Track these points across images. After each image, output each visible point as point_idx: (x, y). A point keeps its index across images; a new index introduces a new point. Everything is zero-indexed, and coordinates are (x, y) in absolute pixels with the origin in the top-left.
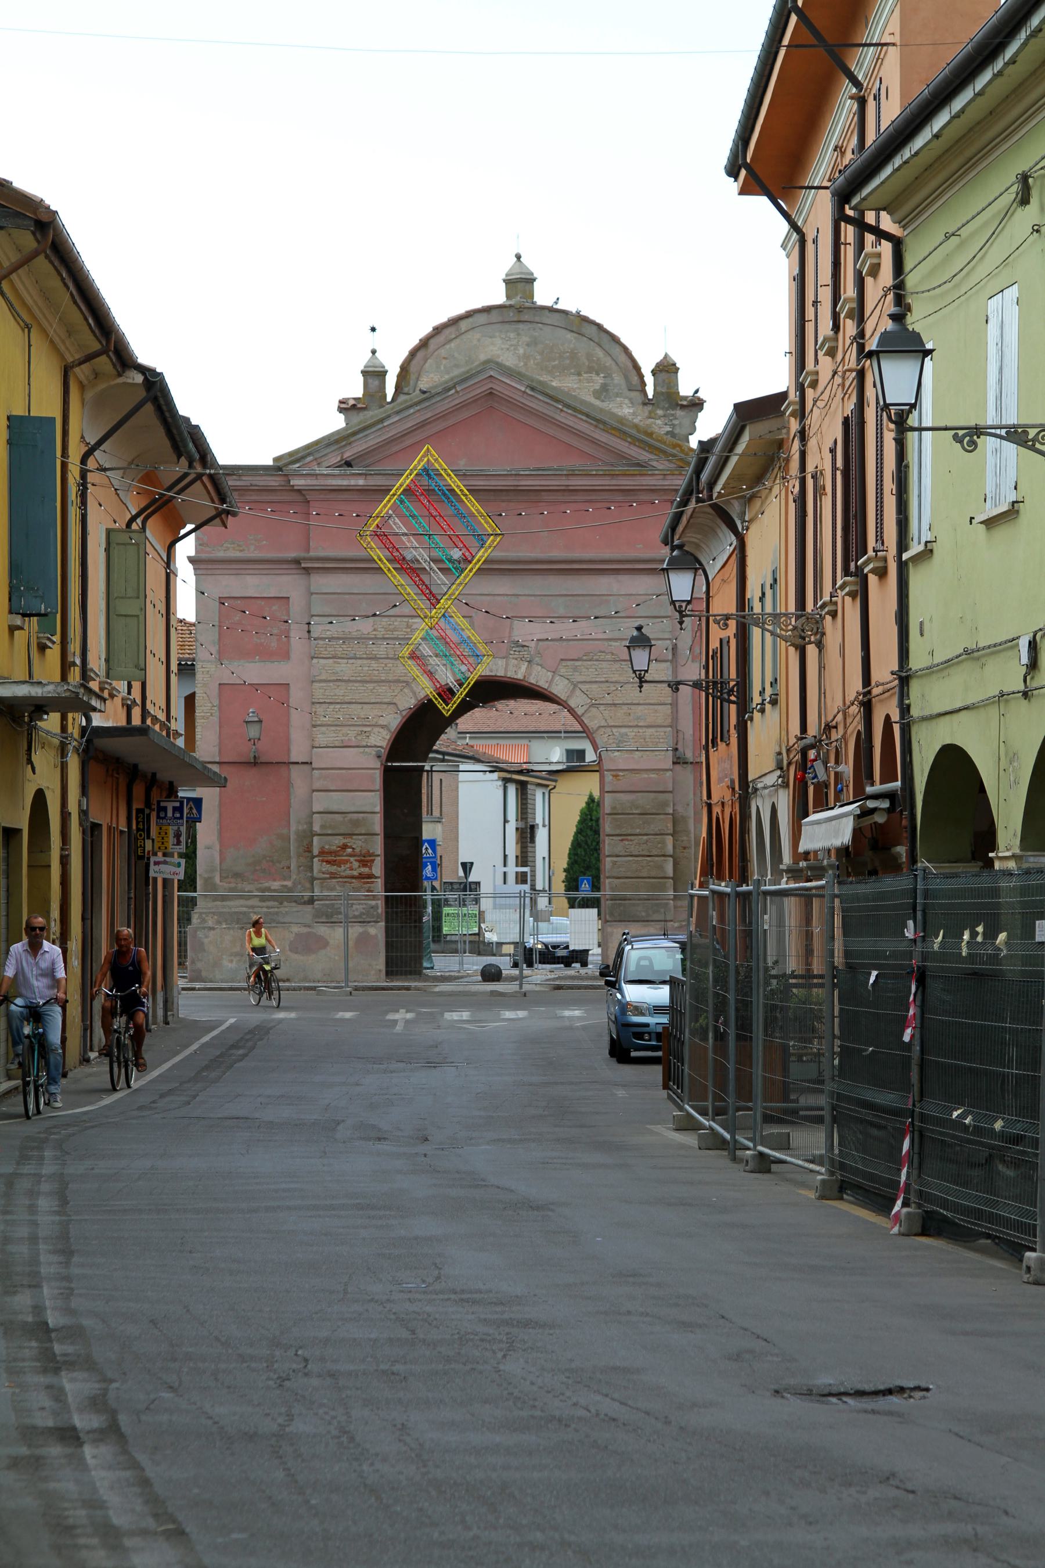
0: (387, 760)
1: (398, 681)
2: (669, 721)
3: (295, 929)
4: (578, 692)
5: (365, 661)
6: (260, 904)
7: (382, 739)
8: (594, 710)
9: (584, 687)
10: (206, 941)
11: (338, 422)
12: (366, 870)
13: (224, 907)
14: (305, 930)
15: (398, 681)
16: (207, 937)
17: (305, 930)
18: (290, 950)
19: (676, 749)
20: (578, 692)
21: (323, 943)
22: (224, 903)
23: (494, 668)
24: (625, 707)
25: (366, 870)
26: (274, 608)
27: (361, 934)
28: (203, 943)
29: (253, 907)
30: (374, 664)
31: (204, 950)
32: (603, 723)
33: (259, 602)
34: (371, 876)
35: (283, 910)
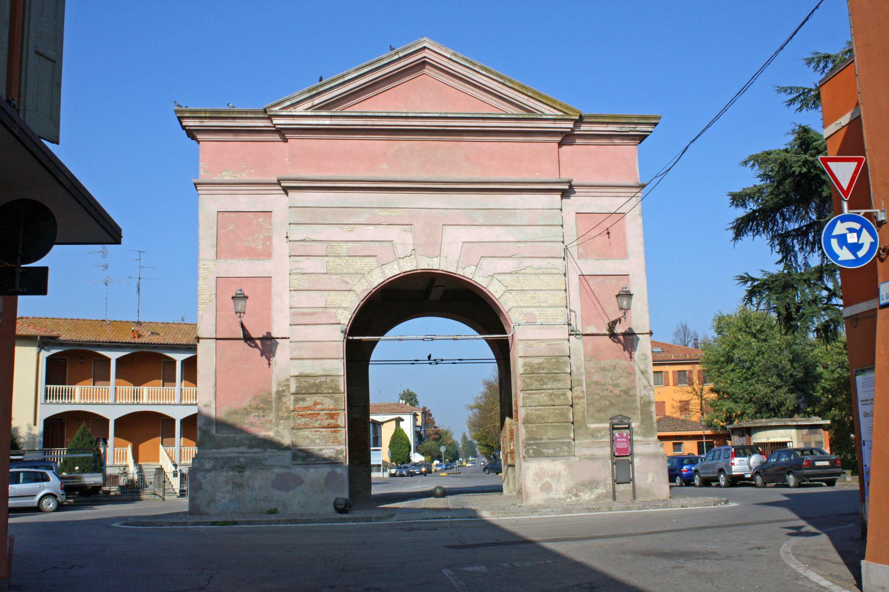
0: (349, 335)
1: (357, 273)
2: (564, 303)
3: (277, 470)
4: (495, 281)
5: (331, 259)
6: (249, 450)
7: (346, 318)
8: (508, 295)
9: (500, 277)
10: (203, 481)
11: (844, 247)
12: (332, 421)
13: (220, 453)
14: (287, 471)
15: (357, 273)
16: (205, 478)
17: (287, 471)
18: (272, 487)
19: (569, 325)
20: (495, 281)
21: (299, 481)
22: (220, 450)
23: (431, 263)
24: (531, 293)
25: (332, 421)
26: (261, 219)
27: (330, 473)
28: (200, 483)
29: (243, 453)
30: (338, 261)
31: (202, 489)
32: (515, 305)
33: (249, 215)
34: (337, 426)
35: (267, 455)
